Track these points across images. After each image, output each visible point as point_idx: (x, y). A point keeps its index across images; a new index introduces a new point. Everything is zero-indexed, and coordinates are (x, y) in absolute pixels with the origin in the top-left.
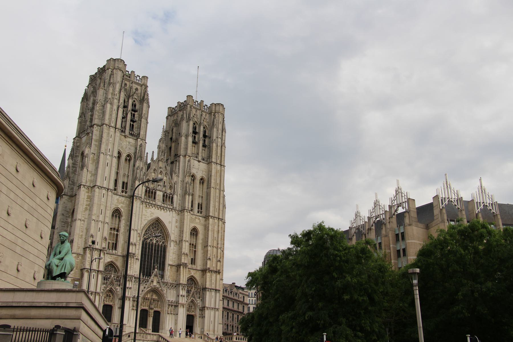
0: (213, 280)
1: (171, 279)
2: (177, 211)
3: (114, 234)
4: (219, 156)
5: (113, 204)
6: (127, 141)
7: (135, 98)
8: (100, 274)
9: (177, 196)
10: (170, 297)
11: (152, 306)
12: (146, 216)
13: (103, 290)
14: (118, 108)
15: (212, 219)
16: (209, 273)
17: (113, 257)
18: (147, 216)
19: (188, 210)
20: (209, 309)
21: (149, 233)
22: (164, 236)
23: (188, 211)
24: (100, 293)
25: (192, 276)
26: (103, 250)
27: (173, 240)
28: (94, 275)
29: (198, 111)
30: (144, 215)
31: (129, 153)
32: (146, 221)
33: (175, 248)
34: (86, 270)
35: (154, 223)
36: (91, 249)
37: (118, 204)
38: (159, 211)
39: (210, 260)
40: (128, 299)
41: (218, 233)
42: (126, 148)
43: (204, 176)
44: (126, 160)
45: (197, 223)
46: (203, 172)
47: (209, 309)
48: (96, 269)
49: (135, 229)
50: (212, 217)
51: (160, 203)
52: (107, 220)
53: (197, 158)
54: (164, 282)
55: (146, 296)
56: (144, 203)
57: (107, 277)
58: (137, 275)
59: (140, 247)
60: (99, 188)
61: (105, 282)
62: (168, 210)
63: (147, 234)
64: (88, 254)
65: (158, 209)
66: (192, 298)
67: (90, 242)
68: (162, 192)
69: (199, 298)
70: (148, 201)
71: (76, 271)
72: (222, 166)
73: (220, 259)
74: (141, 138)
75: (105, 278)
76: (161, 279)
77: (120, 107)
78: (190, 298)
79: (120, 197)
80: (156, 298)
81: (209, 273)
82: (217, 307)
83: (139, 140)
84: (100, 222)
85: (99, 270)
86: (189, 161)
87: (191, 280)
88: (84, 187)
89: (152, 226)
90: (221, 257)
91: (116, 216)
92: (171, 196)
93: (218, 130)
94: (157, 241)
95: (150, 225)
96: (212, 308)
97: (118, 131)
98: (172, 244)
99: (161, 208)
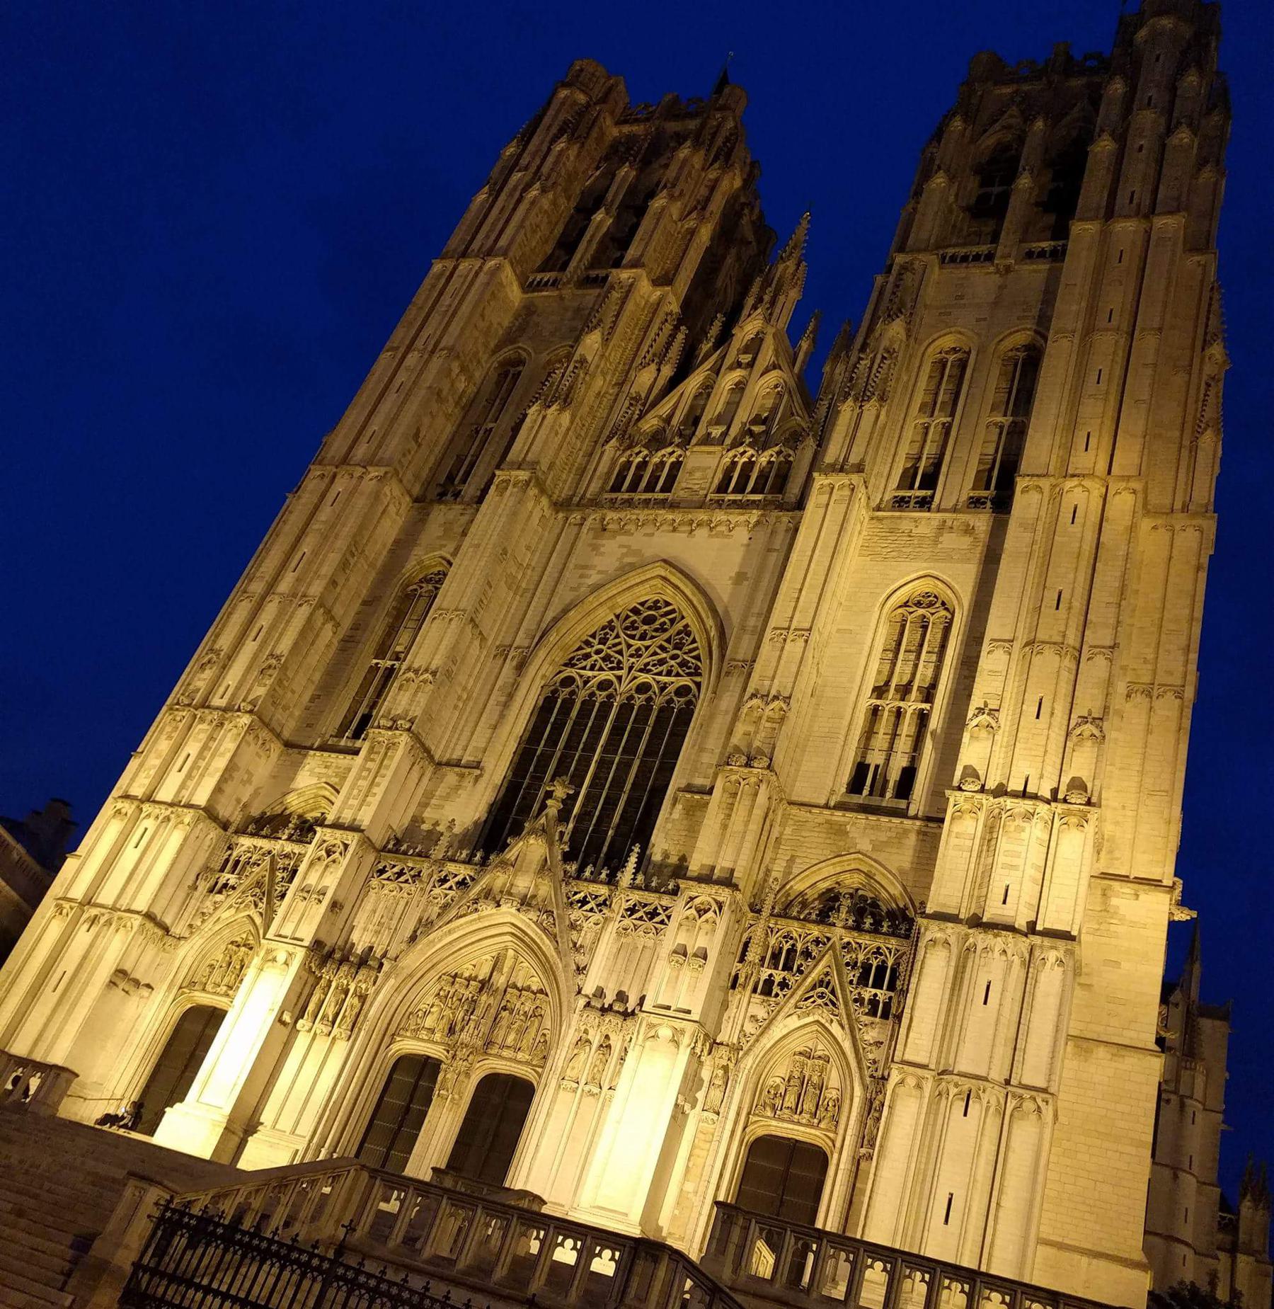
18: (598, 568)
21: (598, 652)
22: (698, 658)
35: (642, 604)
38: (681, 536)
45: (948, 557)
63: (587, 656)
65: (674, 530)
76: (573, 868)
94: (644, 688)
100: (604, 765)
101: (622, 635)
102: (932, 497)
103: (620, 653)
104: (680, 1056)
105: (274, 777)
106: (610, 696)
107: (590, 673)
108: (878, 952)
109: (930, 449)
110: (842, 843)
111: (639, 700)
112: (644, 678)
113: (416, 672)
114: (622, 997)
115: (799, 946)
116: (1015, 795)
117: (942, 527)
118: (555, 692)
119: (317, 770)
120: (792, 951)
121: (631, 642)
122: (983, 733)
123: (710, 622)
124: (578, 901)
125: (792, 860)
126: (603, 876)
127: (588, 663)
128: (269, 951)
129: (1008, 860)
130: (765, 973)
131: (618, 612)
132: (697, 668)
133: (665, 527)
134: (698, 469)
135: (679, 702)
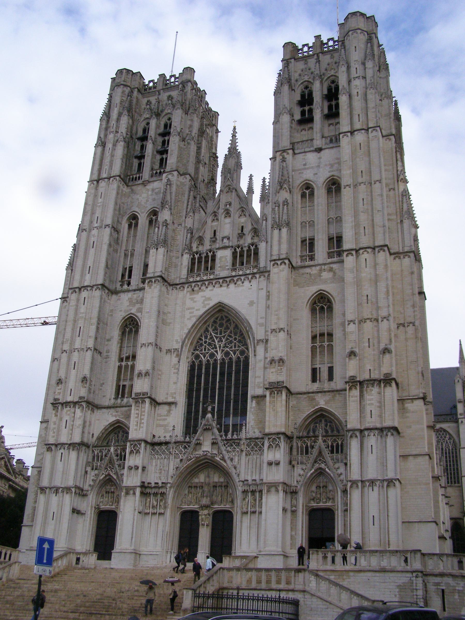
0: (372, 404)
1: (258, 428)
2: (266, 275)
3: (127, 366)
4: (360, 112)
5: (121, 311)
6: (148, 190)
7: (169, 113)
8: (73, 450)
9: (267, 242)
10: (249, 474)
11: (205, 501)
12: (192, 310)
13: (93, 480)
14: (114, 145)
15: (352, 255)
16: (356, 388)
17: (121, 411)
19: (279, 260)
20: (360, 484)
21: (205, 342)
22: (244, 338)
23: (279, 262)
24: (73, 487)
25: (321, 409)
26: (80, 402)
27: (262, 338)
28: (62, 453)
29: (309, 60)
30: (189, 309)
31: (154, 207)
32: (194, 320)
34: (48, 446)
35: (217, 319)
36: (57, 405)
37: (131, 308)
38: (224, 288)
39: (355, 355)
40: (131, 492)
41: (376, 282)
43: (335, 173)
44: (151, 222)
45: (325, 282)
46: (332, 166)
47: (360, 484)
48: (66, 442)
49: (150, 341)
50: (352, 250)
51: (224, 274)
52: (91, 344)
53: (313, 146)
54: (231, 440)
55: (196, 480)
56: (186, 286)
57: (102, 454)
58: (165, 437)
60: (76, 292)
61: (99, 464)
62: (247, 279)
63: (201, 345)
64: (54, 416)
65: (221, 286)
66: (317, 466)
67: (56, 393)
68: (229, 249)
69: (342, 461)
70: (198, 279)
72: (370, 130)
73: (389, 346)
74: (169, 170)
76: (223, 433)
77: (120, 140)
78: (309, 465)
79: (134, 294)
80: (222, 480)
81: (356, 388)
82: (391, 475)
83: (164, 175)
84: (76, 351)
85: (72, 442)
86: (284, 160)
87: (326, 421)
88: (65, 302)
89: (212, 325)
90: (390, 340)
91: (131, 331)
92: (252, 248)
93: (349, 68)
94: (227, 354)
96: (372, 482)
97: (115, 180)
98: (260, 349)
99: (227, 282)
100: (221, 388)
102: (314, 255)
104: (280, 494)
105: (98, 420)
110: (314, 404)
117: (321, 270)
119: (114, 414)
120: (307, 447)
127: (203, 347)
129: (372, 402)
131: (207, 324)
133: (217, 286)
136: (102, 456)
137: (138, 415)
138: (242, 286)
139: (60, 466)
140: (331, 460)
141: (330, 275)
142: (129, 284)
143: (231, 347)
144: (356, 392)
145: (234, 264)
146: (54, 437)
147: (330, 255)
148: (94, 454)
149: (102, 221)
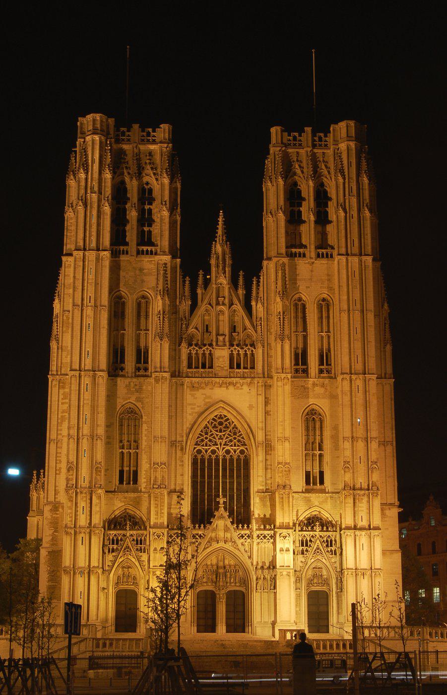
6: (135, 268)
12: (193, 406)
17: (130, 498)
21: (206, 438)
22: (243, 438)
30: (190, 404)
32: (196, 416)
33: (268, 457)
35: (216, 416)
42: (136, 281)
59: (186, 469)
63: (202, 440)
65: (221, 386)
71: (55, 535)
75: (113, 540)
89: (212, 423)
94: (228, 452)
95: (208, 422)
100: (224, 483)
101: (212, 430)
102: (307, 368)
103: (214, 438)
105: (107, 504)
106: (217, 456)
107: (206, 448)
108: (329, 537)
109: (301, 346)
111: (228, 457)
112: (228, 448)
113: (158, 464)
114: (264, 563)
115: (308, 539)
116: (358, 489)
117: (314, 385)
118: (196, 456)
120: (307, 540)
121: (217, 433)
122: (347, 470)
123: (246, 426)
124: (240, 536)
125: (298, 510)
126: (245, 527)
127: (204, 443)
128: (153, 572)
130: (301, 548)
132: (244, 442)
133: (216, 385)
134: (220, 357)
135: (242, 457)
136: (117, 540)
137: (158, 505)
138: (241, 389)
139: (82, 550)
140: (328, 551)
141: (322, 390)
142: (122, 369)
143: (232, 446)
144: (350, 500)
145: (231, 367)
146: (71, 521)
147: (321, 371)
148: (109, 538)
149: (95, 301)
